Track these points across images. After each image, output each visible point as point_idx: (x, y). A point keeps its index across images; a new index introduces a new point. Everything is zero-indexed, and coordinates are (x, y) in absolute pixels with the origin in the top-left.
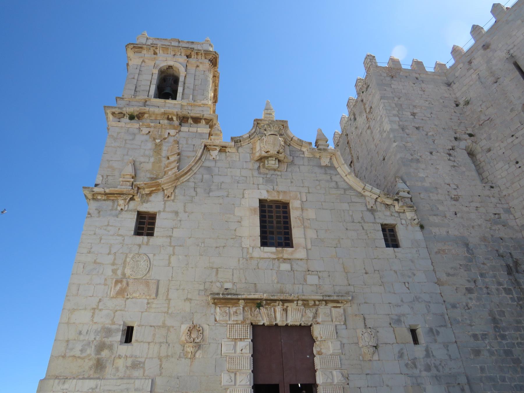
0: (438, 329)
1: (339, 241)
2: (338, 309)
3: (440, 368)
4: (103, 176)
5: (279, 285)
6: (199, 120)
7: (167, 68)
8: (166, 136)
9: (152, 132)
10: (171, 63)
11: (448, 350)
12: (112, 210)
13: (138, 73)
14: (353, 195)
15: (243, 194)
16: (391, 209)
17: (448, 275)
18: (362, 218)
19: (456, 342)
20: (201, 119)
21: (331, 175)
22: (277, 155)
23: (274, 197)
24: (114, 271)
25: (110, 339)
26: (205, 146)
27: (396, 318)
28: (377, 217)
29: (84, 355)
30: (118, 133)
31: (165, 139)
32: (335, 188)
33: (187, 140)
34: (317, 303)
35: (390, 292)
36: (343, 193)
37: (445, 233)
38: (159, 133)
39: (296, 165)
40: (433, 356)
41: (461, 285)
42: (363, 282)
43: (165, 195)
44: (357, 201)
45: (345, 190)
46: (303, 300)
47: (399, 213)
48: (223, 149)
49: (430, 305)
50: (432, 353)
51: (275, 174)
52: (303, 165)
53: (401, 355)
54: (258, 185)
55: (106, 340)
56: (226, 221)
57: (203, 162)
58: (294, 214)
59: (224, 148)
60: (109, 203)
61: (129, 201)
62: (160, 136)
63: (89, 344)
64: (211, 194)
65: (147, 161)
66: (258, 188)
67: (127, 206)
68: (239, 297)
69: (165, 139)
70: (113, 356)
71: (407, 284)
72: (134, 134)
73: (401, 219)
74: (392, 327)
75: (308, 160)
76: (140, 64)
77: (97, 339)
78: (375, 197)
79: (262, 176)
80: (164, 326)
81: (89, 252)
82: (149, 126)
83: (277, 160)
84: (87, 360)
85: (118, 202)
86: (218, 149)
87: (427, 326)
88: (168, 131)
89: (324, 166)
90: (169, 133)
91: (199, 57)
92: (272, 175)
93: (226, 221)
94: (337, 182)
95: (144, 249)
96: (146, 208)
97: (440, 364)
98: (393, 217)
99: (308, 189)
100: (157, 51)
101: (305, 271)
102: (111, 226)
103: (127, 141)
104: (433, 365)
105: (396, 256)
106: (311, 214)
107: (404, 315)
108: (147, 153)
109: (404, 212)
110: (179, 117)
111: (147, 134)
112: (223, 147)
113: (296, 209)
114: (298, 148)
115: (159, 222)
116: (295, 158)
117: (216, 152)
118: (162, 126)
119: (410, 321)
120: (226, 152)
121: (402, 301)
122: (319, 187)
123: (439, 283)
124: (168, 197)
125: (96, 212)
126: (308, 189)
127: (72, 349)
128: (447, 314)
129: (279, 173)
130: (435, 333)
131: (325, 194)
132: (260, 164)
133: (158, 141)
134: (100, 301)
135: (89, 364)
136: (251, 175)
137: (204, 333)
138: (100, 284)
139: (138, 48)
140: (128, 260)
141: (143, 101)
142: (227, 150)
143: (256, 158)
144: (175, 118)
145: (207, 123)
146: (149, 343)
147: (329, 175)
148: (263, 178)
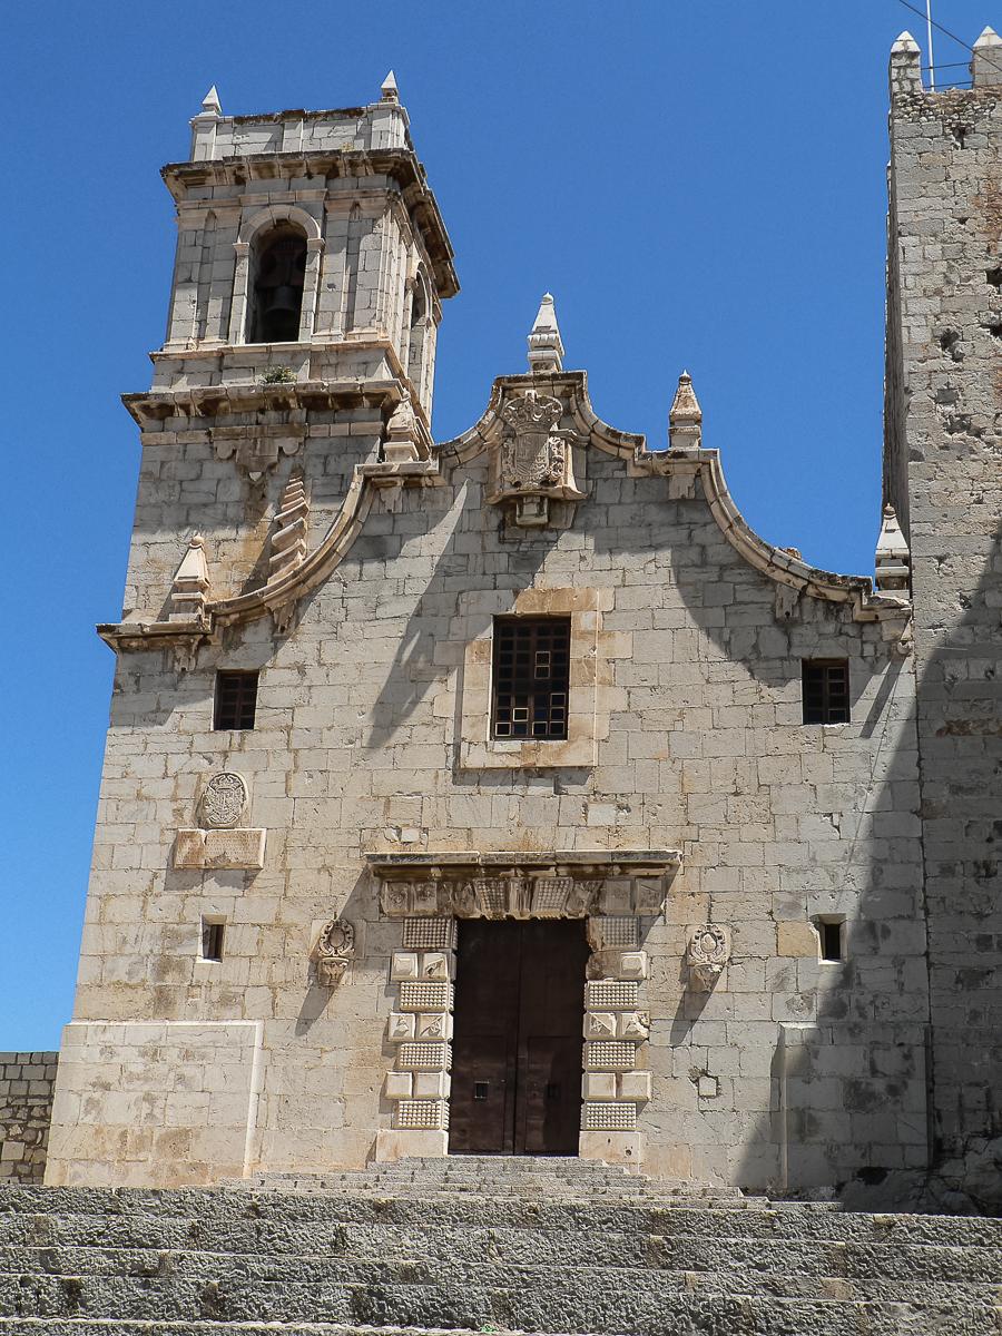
0: (890, 924)
1: (681, 714)
2: (649, 883)
3: (870, 1011)
4: (137, 587)
5: (523, 830)
6: (353, 400)
7: (275, 226)
8: (275, 459)
9: (241, 451)
10: (281, 211)
11: (900, 972)
12: (163, 672)
13: (199, 259)
14: (740, 583)
15: (457, 605)
16: (842, 614)
17: (957, 789)
18: (755, 647)
19: (927, 954)
20: (360, 396)
21: (692, 527)
22: (541, 489)
23: (532, 607)
24: (178, 813)
25: (179, 951)
26: (367, 479)
27: (789, 898)
28: (796, 640)
29: (133, 982)
30: (163, 464)
31: (272, 466)
32: (696, 566)
33: (325, 464)
34: (602, 868)
35: (787, 840)
36: (717, 579)
37: (982, 675)
38: (257, 453)
39: (599, 505)
40: (859, 984)
41: (986, 815)
42: (726, 816)
43: (274, 627)
44: (750, 599)
45: (723, 568)
46: (568, 865)
47: (862, 624)
48: (412, 481)
49: (884, 867)
50: (858, 975)
51: (542, 538)
52: (620, 503)
53: (781, 983)
54: (495, 575)
55: (172, 953)
56: (412, 681)
57: (363, 524)
58: (577, 650)
59: (416, 479)
60: (157, 657)
61: (198, 646)
62: (261, 460)
63: (142, 961)
64: (380, 612)
65: (233, 537)
66: (495, 584)
67: (194, 661)
68: (427, 862)
69: (272, 466)
70: (187, 984)
71: (835, 817)
72: (201, 462)
73: (863, 642)
74: (773, 920)
75: (636, 485)
76: (203, 227)
77: (155, 951)
78: (801, 583)
79: (507, 547)
80: (278, 924)
81: (125, 775)
82: (234, 436)
83: (546, 500)
84: (140, 991)
85: (174, 653)
86: (400, 482)
87: (863, 918)
88: (278, 443)
89: (678, 500)
90: (281, 449)
91: (361, 170)
92: (533, 543)
93: (412, 681)
94: (703, 547)
95: (238, 766)
96: (236, 661)
97: (872, 1002)
98: (843, 638)
99: (624, 576)
100: (244, 173)
101: (588, 796)
102: (163, 711)
103: (185, 485)
104: (853, 1004)
105: (825, 746)
106: (622, 646)
107: (811, 893)
108: (231, 512)
109: (876, 622)
110: (303, 397)
111: (228, 459)
112: (410, 476)
113: (584, 634)
114: (613, 451)
115: (263, 695)
116: (600, 482)
117: (396, 492)
118: (262, 432)
119: (826, 907)
120: (421, 488)
121: (814, 859)
122: (652, 567)
123: (925, 811)
124: (283, 629)
125: (132, 680)
126: (624, 576)
127: (112, 972)
128: (924, 890)
129: (551, 536)
130: (879, 932)
131: (666, 586)
132: (504, 512)
133: (255, 476)
134: (155, 876)
135: (143, 998)
136: (479, 550)
137: (357, 939)
138: (151, 843)
139: (195, 175)
140: (203, 785)
141: (215, 355)
142: (426, 481)
143: (492, 500)
144: (293, 403)
145: (375, 406)
146: (251, 957)
147: (687, 526)
148: (509, 556)
